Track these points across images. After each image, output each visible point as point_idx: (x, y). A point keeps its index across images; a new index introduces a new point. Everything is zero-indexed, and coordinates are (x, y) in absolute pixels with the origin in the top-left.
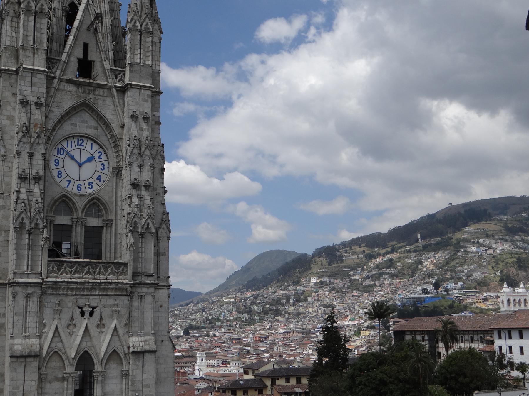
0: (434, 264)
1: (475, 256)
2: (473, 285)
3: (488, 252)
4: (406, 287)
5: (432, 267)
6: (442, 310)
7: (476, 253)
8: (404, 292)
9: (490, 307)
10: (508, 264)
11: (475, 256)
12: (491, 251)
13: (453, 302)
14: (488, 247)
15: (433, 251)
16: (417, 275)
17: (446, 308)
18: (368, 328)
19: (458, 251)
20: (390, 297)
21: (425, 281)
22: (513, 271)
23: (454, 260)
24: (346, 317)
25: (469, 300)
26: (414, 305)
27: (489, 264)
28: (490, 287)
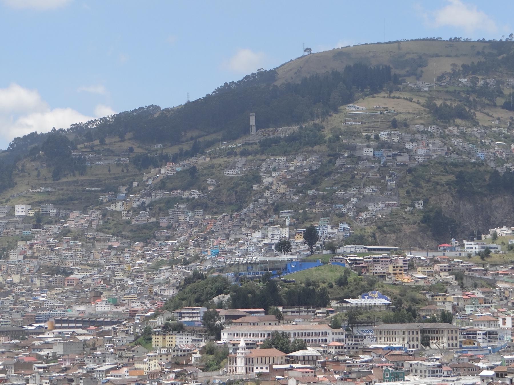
0: (289, 183)
1: (372, 167)
2: (369, 230)
3: (399, 159)
4: (227, 231)
5: (283, 188)
6: (324, 289)
7: (375, 161)
8: (224, 243)
9: (421, 283)
10: (439, 187)
11: (372, 167)
12: (403, 159)
13: (347, 272)
14: (398, 148)
15: (283, 155)
16: (251, 206)
17: (331, 286)
18: (167, 329)
19: (336, 156)
20: (192, 252)
21: (269, 220)
22: (446, 202)
23: (328, 174)
24: (98, 295)
25: (379, 269)
26: (266, 278)
27: (400, 185)
28: (402, 234)
